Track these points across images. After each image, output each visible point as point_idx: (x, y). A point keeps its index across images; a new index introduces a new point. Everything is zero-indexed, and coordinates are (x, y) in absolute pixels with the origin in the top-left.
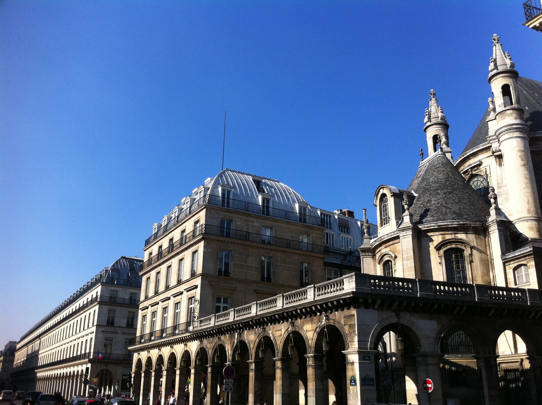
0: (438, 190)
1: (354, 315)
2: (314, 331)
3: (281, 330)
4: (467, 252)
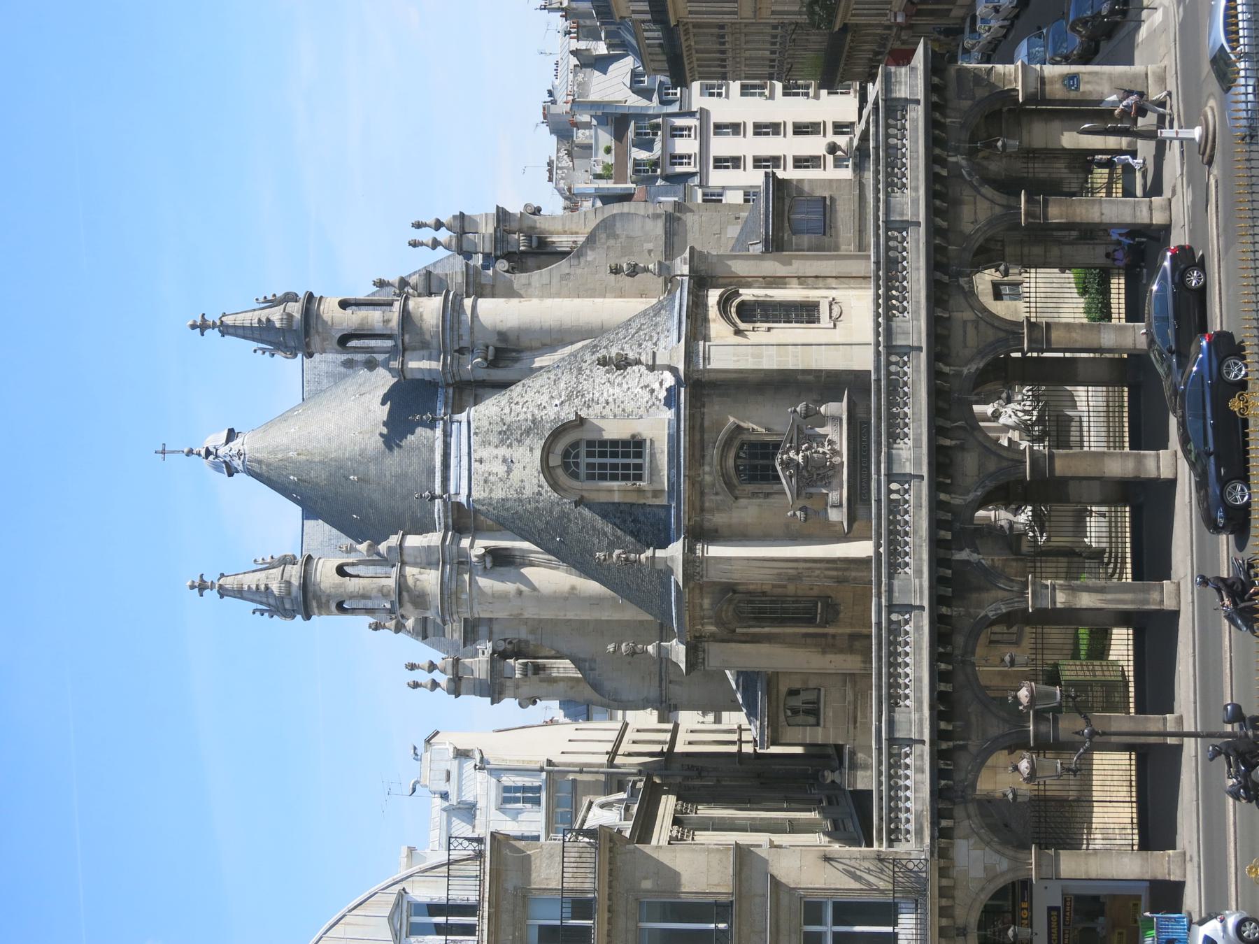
2: (978, 197)
3: (965, 322)
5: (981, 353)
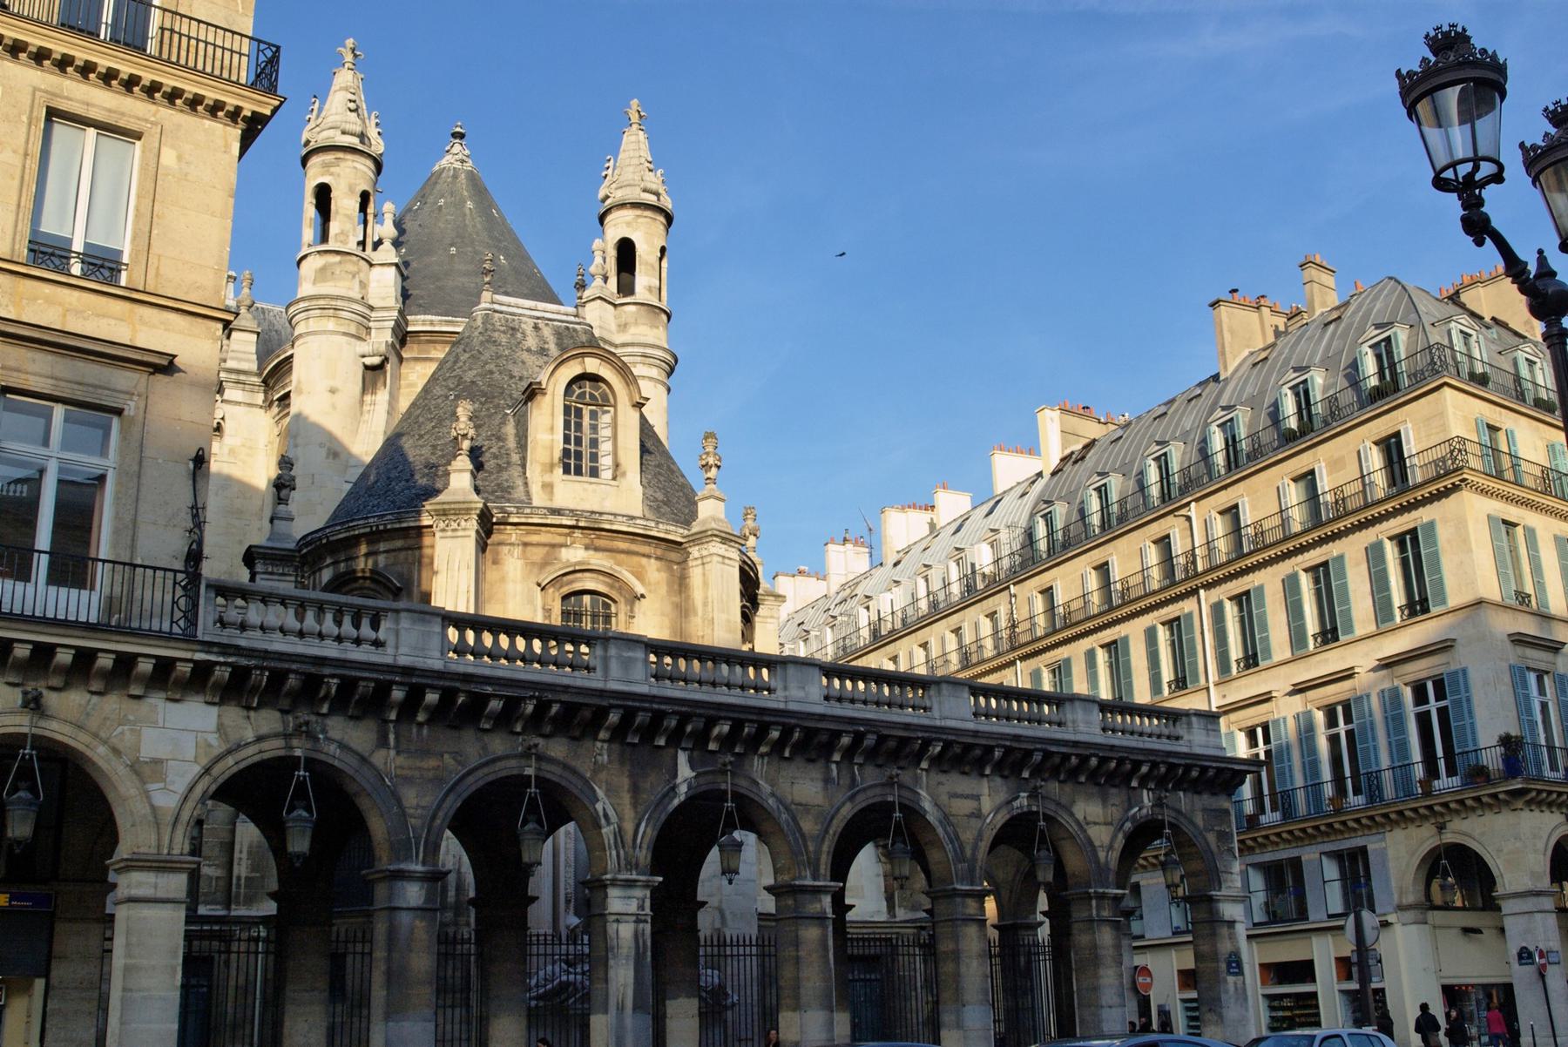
1: (1227, 812)
2: (1112, 829)
3: (977, 798)
5: (946, 818)
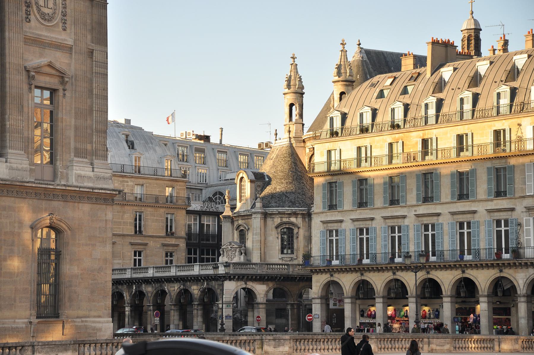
0: (282, 179)
3: (175, 287)
4: (295, 231)
5: (169, 291)
